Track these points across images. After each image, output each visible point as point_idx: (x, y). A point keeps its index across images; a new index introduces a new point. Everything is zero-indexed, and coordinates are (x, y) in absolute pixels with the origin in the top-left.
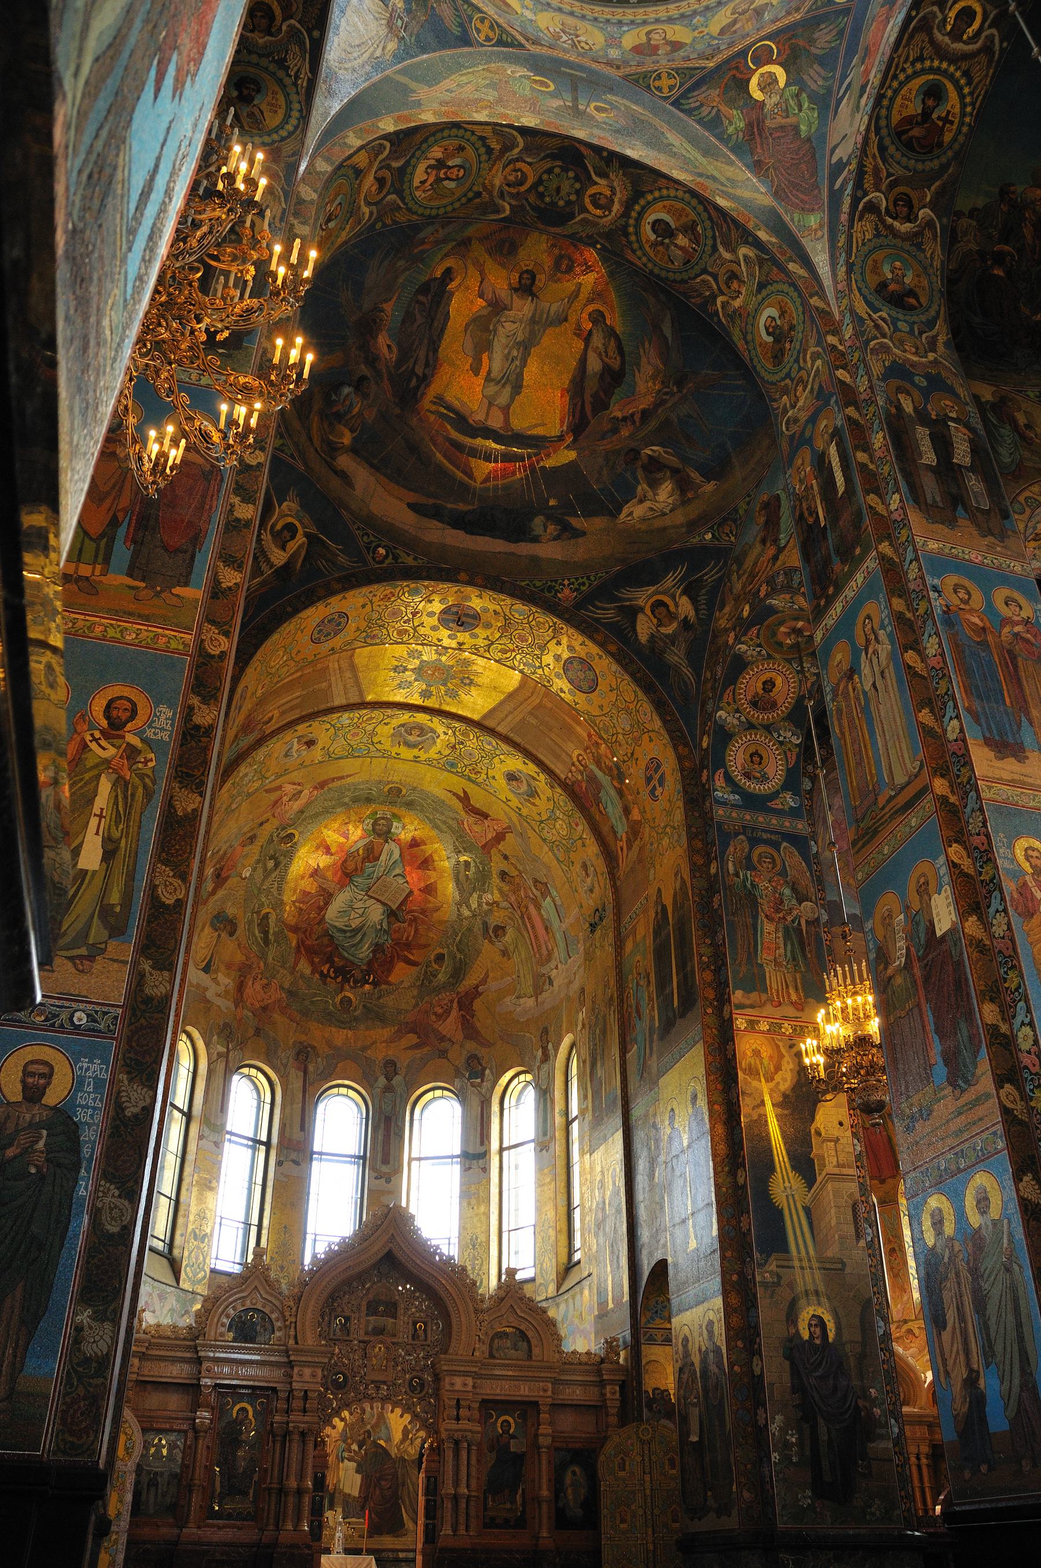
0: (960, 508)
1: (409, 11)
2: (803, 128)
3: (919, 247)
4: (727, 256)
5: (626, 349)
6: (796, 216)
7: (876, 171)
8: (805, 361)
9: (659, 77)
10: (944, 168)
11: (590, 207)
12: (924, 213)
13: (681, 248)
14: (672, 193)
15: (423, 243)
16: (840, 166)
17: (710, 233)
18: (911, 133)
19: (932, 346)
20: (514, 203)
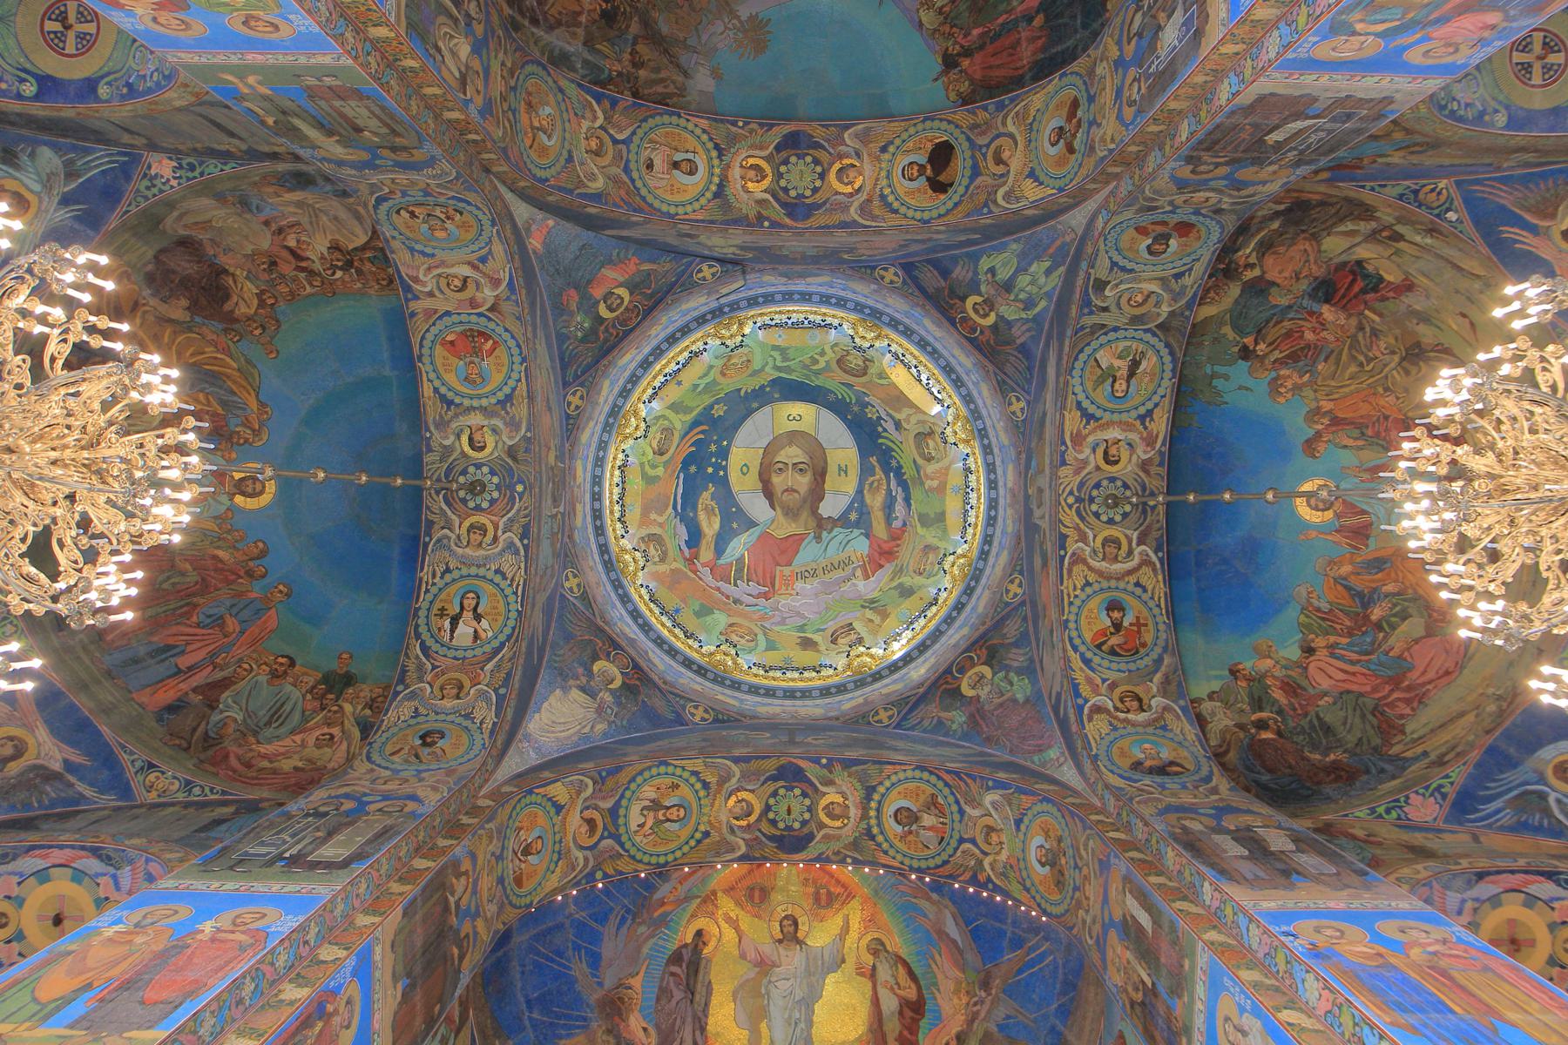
0: (1295, 876)
1: (619, 704)
2: (1020, 697)
3: (1164, 728)
4: (976, 813)
5: (918, 971)
6: (1036, 759)
7: (1089, 681)
8: (1081, 858)
9: (877, 713)
10: (1159, 661)
11: (826, 820)
12: (1157, 702)
13: (930, 828)
14: (902, 775)
15: (663, 904)
16: (1059, 695)
17: (951, 799)
18: (1110, 643)
19: (1215, 791)
20: (747, 836)
